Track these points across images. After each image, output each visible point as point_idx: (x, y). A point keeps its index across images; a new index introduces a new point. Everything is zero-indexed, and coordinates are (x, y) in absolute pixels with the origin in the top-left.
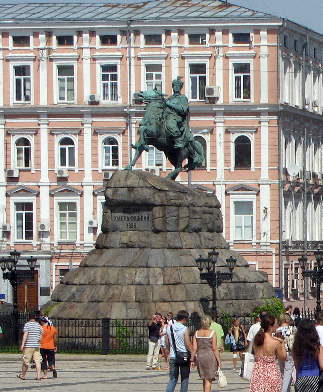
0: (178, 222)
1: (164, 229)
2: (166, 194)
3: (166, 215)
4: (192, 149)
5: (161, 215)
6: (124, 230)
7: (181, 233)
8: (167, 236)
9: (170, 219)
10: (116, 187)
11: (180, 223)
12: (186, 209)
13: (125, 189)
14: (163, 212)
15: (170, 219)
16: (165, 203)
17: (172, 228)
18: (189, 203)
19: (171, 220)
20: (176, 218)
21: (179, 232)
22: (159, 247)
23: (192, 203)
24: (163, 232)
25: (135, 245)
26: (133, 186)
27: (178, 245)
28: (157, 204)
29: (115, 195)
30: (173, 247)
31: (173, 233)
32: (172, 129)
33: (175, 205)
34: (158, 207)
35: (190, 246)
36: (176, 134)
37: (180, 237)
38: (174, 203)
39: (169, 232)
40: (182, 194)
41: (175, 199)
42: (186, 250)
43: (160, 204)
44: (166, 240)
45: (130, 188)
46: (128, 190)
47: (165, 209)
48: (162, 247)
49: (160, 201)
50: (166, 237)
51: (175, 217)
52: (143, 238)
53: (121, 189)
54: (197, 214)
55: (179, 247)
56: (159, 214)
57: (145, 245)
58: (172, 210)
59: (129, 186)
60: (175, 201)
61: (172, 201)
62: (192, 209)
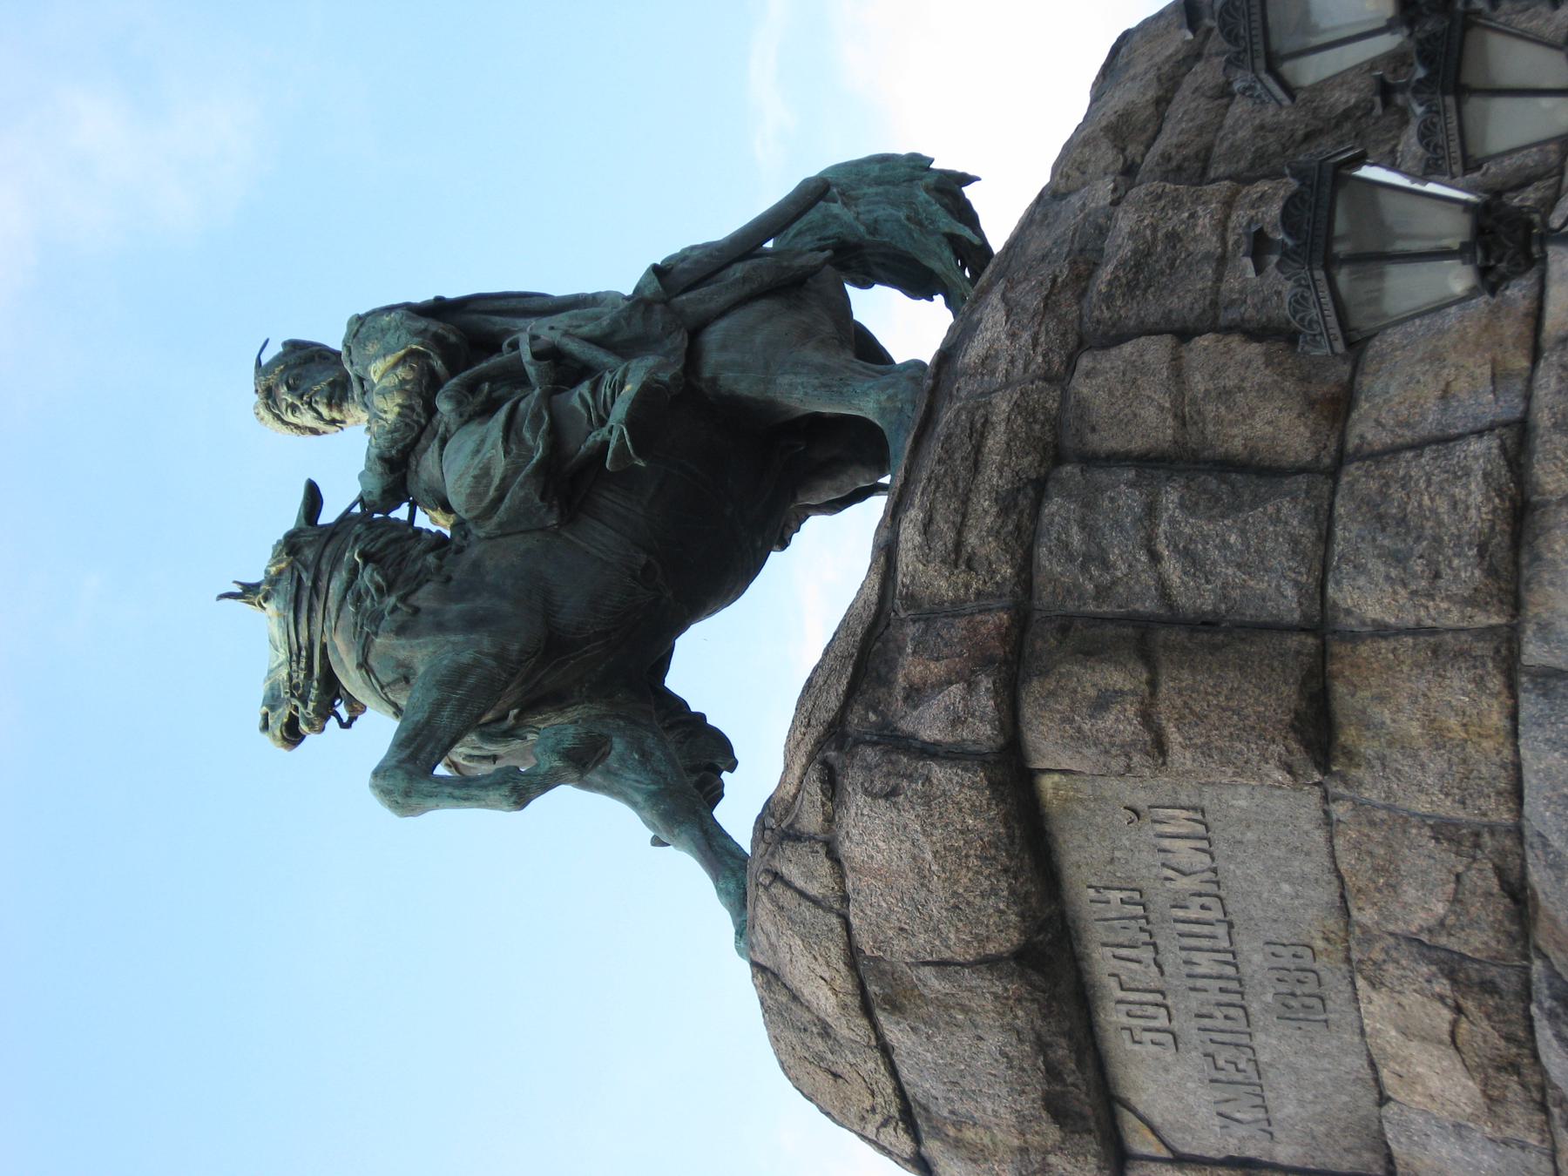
0: (1226, 466)
1: (1293, 642)
2: (911, 599)
3: (1133, 619)
4: (738, 270)
5: (1117, 679)
6: (1359, 1063)
7: (1353, 442)
8: (1373, 611)
9: (1172, 569)
10: (894, 1111)
11: (1237, 446)
12: (1088, 375)
13: (894, 1032)
14: (1091, 652)
15: (1172, 569)
16: (995, 620)
17: (1280, 557)
18: (1026, 337)
19: (1187, 555)
20: (1170, 498)
21: (1342, 458)
22: (1496, 719)
23: (1034, 302)
24: (1323, 654)
25: (1489, 987)
26: (836, 953)
27: (1476, 485)
28: (982, 731)
29: (969, 1134)
30: (1501, 540)
31: (1339, 533)
32: (485, 473)
33: (1023, 502)
34: (1028, 712)
35: (1511, 328)
36: (527, 435)
37: (1394, 451)
38: (1004, 512)
39: (1331, 590)
40: (947, 416)
41: (965, 501)
42: (1548, 381)
43: (985, 683)
44: (1417, 631)
45: (873, 989)
46: (895, 1007)
47: (1065, 625)
48: (1496, 683)
49: (956, 689)
50: (1382, 631)
51: (1151, 510)
52: (1410, 893)
53: (905, 1073)
54: (1173, 238)
55: (1504, 475)
56: (1102, 703)
57: (1494, 884)
58: (1076, 538)
59: (853, 1002)
60: (983, 503)
61: (972, 539)
62: (1108, 298)
